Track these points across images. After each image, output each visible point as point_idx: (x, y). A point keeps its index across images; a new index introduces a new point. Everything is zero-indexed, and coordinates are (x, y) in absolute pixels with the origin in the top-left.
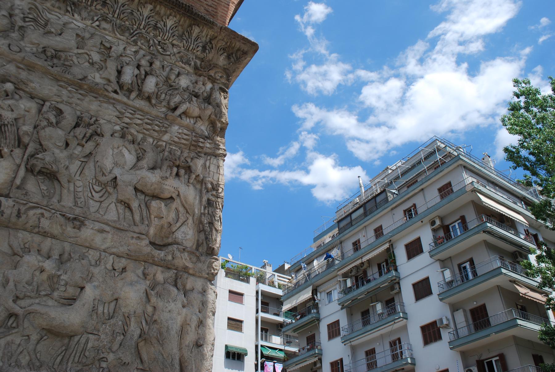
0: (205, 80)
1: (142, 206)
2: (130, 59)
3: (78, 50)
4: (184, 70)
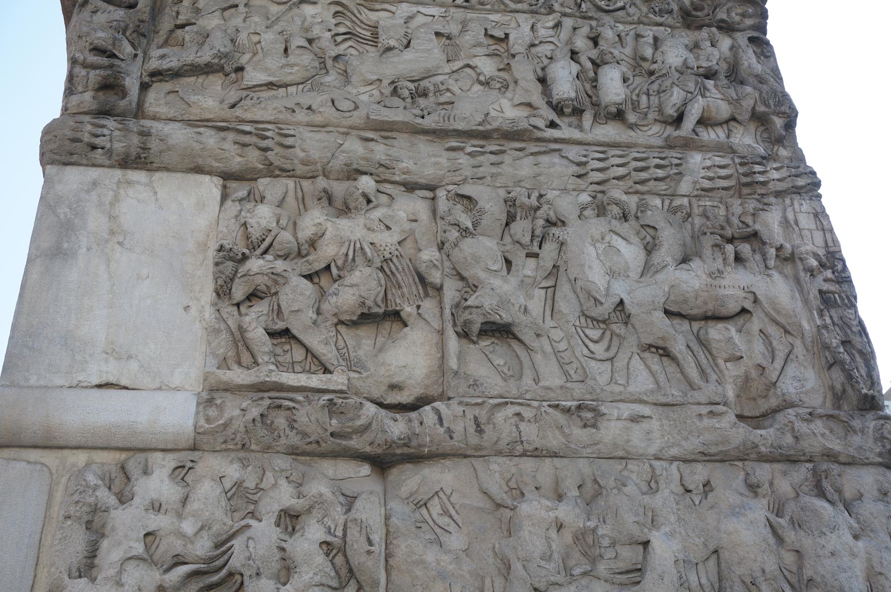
0: (714, 34)
1: (691, 345)
3: (451, 64)
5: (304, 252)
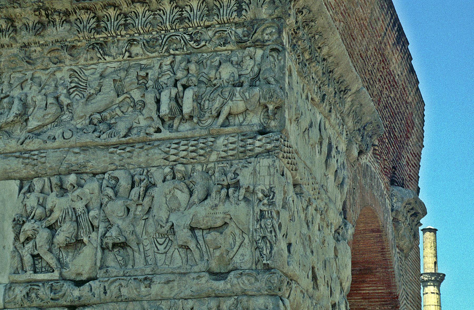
2: (168, 77)
4: (227, 52)
5: (48, 215)
